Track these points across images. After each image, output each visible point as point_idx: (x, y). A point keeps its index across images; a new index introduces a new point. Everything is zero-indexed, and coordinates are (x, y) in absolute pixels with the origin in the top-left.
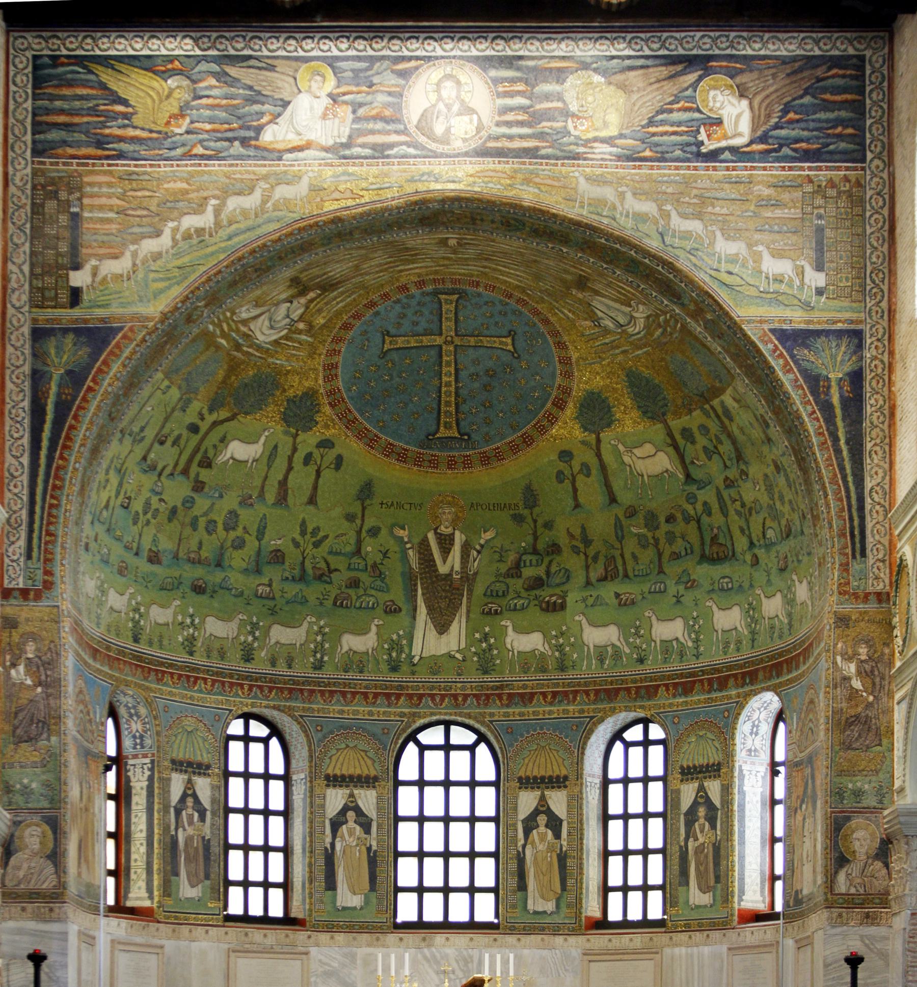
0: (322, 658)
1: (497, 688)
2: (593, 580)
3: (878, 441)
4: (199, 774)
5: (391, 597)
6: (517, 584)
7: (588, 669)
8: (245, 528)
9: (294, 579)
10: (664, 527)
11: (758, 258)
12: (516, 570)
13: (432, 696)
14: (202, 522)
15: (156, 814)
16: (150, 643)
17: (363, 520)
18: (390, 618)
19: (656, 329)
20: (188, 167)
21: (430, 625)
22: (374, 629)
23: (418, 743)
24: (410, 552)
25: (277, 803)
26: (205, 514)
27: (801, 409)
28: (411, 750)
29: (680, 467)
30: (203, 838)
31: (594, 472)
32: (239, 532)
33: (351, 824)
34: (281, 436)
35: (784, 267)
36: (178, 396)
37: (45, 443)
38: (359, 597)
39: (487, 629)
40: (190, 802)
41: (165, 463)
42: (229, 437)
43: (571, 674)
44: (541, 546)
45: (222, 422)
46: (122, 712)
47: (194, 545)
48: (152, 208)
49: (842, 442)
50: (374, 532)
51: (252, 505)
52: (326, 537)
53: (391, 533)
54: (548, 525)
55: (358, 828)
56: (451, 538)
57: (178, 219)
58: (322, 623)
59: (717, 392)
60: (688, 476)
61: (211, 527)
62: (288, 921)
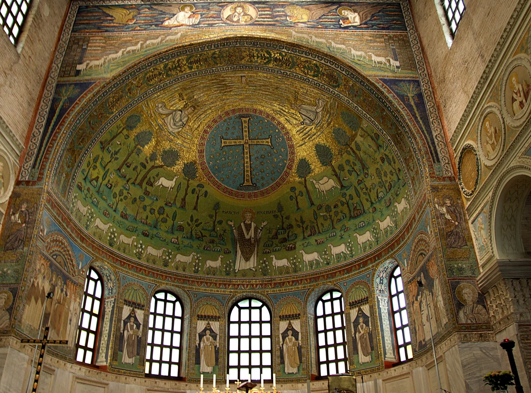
0: (198, 269)
1: (269, 281)
2: (306, 237)
3: (435, 118)
4: (138, 308)
6: (276, 241)
7: (306, 271)
8: (167, 215)
10: (334, 210)
11: (370, 57)
12: (276, 236)
13: (243, 285)
14: (148, 208)
15: (113, 322)
16: (119, 249)
18: (226, 255)
19: (326, 115)
20: (134, 33)
21: (242, 258)
22: (220, 259)
23: (238, 307)
25: (177, 328)
26: (150, 205)
27: (398, 107)
28: (236, 309)
29: (339, 184)
30: (138, 337)
31: (305, 194)
32: (165, 216)
33: (208, 336)
35: (382, 59)
36: (134, 145)
37: (53, 123)
38: (214, 247)
39: (265, 259)
40: (132, 319)
42: (160, 175)
43: (299, 273)
44: (285, 226)
45: (157, 167)
46: (105, 279)
47: (144, 217)
48: (117, 45)
49: (419, 118)
50: (220, 222)
52: (201, 223)
53: (227, 222)
54: (288, 218)
55: (211, 338)
57: (126, 48)
59: (354, 137)
60: (342, 186)
61: (152, 211)
62: (179, 378)
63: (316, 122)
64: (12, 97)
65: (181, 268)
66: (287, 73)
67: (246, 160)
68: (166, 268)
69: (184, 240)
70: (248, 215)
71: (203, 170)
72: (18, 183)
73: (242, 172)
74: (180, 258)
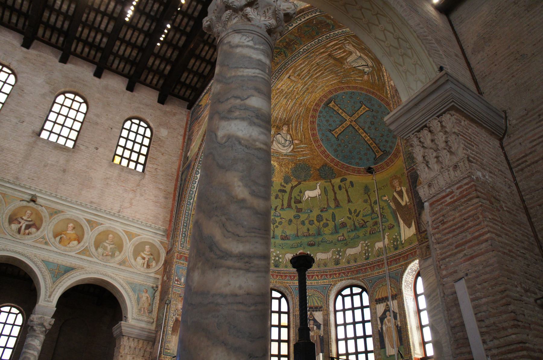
0: (368, 255)
5: (390, 223)
8: (327, 220)
9: (352, 231)
14: (307, 222)
17: (370, 200)
24: (391, 203)
32: (325, 221)
34: (325, 183)
41: (276, 205)
45: (296, 186)
47: (305, 230)
50: (375, 203)
51: (326, 210)
52: (360, 211)
56: (401, 191)
58: (367, 242)
61: (311, 223)
63: (370, 64)
64: (146, 201)
65: (352, 261)
66: (305, 49)
67: (363, 135)
68: (338, 266)
69: (350, 234)
70: (396, 183)
71: (337, 166)
72: (167, 253)
73: (368, 147)
74: (350, 251)
